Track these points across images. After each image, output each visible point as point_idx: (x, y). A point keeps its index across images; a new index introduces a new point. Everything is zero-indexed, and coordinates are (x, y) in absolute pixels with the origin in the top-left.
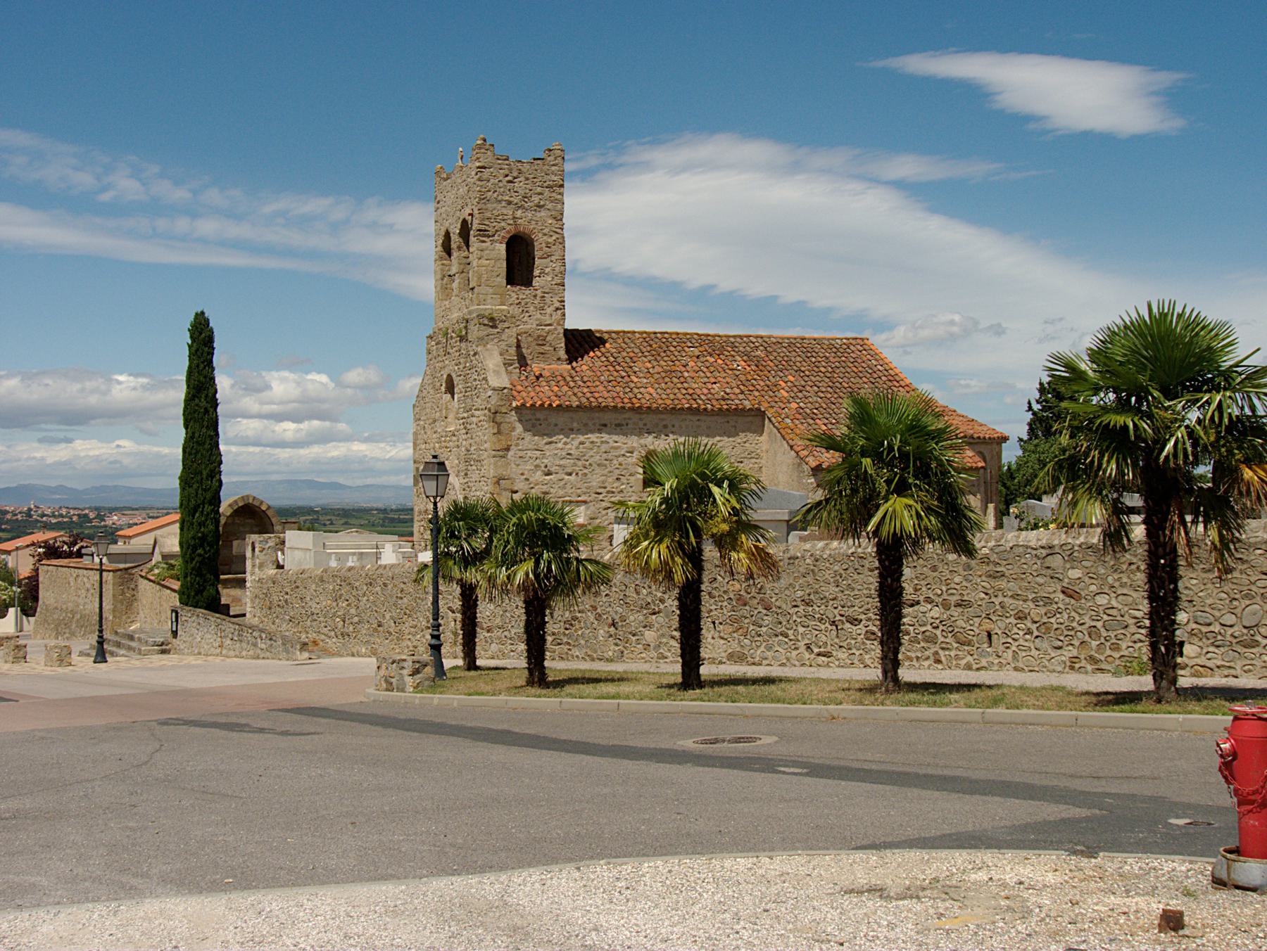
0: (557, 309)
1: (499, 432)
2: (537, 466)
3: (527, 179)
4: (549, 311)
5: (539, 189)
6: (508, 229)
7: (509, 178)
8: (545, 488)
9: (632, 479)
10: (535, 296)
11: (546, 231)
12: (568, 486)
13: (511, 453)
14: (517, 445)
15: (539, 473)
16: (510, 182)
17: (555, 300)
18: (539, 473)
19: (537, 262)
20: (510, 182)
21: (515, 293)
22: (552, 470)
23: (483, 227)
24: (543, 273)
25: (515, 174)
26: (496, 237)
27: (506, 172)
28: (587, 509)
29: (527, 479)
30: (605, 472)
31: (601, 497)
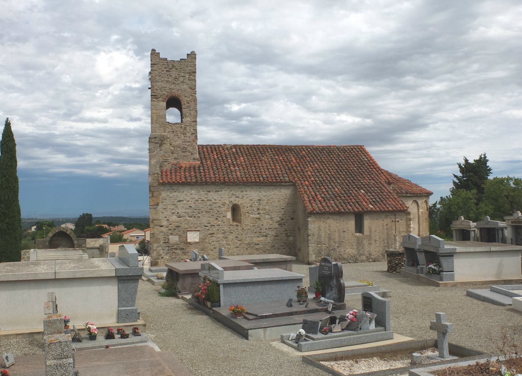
0: (193, 134)
1: (152, 196)
3: (177, 69)
4: (189, 135)
5: (183, 74)
8: (177, 224)
13: (159, 207)
14: (162, 202)
16: (167, 71)
20: (167, 71)
22: (182, 215)
31: (207, 228)
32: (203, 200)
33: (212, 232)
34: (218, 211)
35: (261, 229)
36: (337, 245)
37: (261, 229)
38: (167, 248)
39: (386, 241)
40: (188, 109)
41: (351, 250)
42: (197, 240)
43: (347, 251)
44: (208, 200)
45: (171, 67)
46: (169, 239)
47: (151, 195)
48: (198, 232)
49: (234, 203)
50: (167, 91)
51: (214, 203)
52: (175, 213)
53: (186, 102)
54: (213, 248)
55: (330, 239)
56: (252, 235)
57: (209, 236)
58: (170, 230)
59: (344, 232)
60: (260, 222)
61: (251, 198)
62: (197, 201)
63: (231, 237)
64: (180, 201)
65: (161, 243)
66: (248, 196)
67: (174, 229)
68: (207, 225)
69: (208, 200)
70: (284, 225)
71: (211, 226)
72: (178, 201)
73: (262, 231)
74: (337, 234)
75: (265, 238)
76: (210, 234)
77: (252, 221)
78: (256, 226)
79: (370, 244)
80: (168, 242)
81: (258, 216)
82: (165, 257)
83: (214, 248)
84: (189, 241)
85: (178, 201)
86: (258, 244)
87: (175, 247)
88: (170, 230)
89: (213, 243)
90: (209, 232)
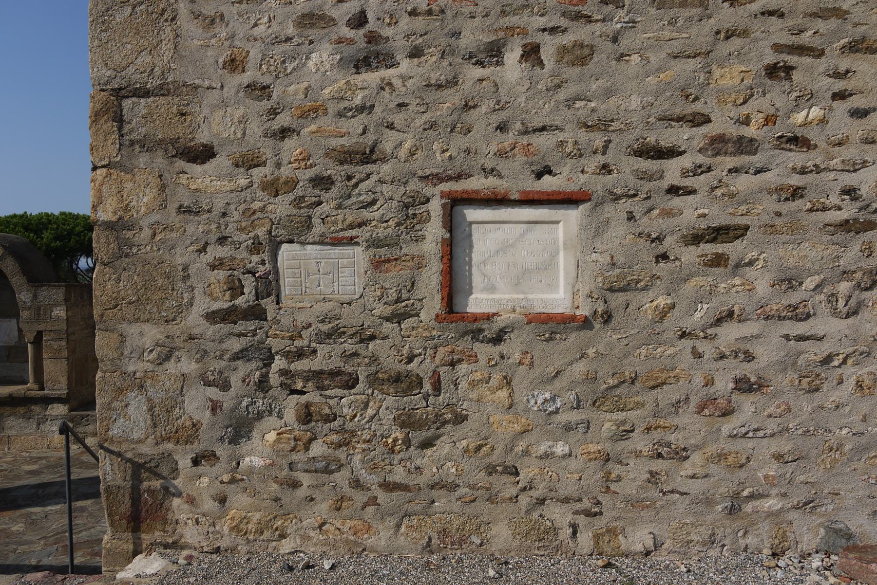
12: (482, 119)
18: (322, 57)
28: (596, 230)
30: (701, 34)
31: (673, 171)
33: (719, 215)
38: (249, 368)
42: (558, 297)
46: (269, 286)
48: (571, 219)
52: (326, 21)
54: (723, 385)
57: (690, 255)
58: (273, 188)
65: (194, 320)
67: (322, 182)
68: (667, 137)
71: (718, 144)
76: (696, 239)
80: (256, 313)
82: (223, 451)
84: (477, 302)
87: (325, 358)
88: (273, 188)
89: (730, 333)
90: (691, 212)
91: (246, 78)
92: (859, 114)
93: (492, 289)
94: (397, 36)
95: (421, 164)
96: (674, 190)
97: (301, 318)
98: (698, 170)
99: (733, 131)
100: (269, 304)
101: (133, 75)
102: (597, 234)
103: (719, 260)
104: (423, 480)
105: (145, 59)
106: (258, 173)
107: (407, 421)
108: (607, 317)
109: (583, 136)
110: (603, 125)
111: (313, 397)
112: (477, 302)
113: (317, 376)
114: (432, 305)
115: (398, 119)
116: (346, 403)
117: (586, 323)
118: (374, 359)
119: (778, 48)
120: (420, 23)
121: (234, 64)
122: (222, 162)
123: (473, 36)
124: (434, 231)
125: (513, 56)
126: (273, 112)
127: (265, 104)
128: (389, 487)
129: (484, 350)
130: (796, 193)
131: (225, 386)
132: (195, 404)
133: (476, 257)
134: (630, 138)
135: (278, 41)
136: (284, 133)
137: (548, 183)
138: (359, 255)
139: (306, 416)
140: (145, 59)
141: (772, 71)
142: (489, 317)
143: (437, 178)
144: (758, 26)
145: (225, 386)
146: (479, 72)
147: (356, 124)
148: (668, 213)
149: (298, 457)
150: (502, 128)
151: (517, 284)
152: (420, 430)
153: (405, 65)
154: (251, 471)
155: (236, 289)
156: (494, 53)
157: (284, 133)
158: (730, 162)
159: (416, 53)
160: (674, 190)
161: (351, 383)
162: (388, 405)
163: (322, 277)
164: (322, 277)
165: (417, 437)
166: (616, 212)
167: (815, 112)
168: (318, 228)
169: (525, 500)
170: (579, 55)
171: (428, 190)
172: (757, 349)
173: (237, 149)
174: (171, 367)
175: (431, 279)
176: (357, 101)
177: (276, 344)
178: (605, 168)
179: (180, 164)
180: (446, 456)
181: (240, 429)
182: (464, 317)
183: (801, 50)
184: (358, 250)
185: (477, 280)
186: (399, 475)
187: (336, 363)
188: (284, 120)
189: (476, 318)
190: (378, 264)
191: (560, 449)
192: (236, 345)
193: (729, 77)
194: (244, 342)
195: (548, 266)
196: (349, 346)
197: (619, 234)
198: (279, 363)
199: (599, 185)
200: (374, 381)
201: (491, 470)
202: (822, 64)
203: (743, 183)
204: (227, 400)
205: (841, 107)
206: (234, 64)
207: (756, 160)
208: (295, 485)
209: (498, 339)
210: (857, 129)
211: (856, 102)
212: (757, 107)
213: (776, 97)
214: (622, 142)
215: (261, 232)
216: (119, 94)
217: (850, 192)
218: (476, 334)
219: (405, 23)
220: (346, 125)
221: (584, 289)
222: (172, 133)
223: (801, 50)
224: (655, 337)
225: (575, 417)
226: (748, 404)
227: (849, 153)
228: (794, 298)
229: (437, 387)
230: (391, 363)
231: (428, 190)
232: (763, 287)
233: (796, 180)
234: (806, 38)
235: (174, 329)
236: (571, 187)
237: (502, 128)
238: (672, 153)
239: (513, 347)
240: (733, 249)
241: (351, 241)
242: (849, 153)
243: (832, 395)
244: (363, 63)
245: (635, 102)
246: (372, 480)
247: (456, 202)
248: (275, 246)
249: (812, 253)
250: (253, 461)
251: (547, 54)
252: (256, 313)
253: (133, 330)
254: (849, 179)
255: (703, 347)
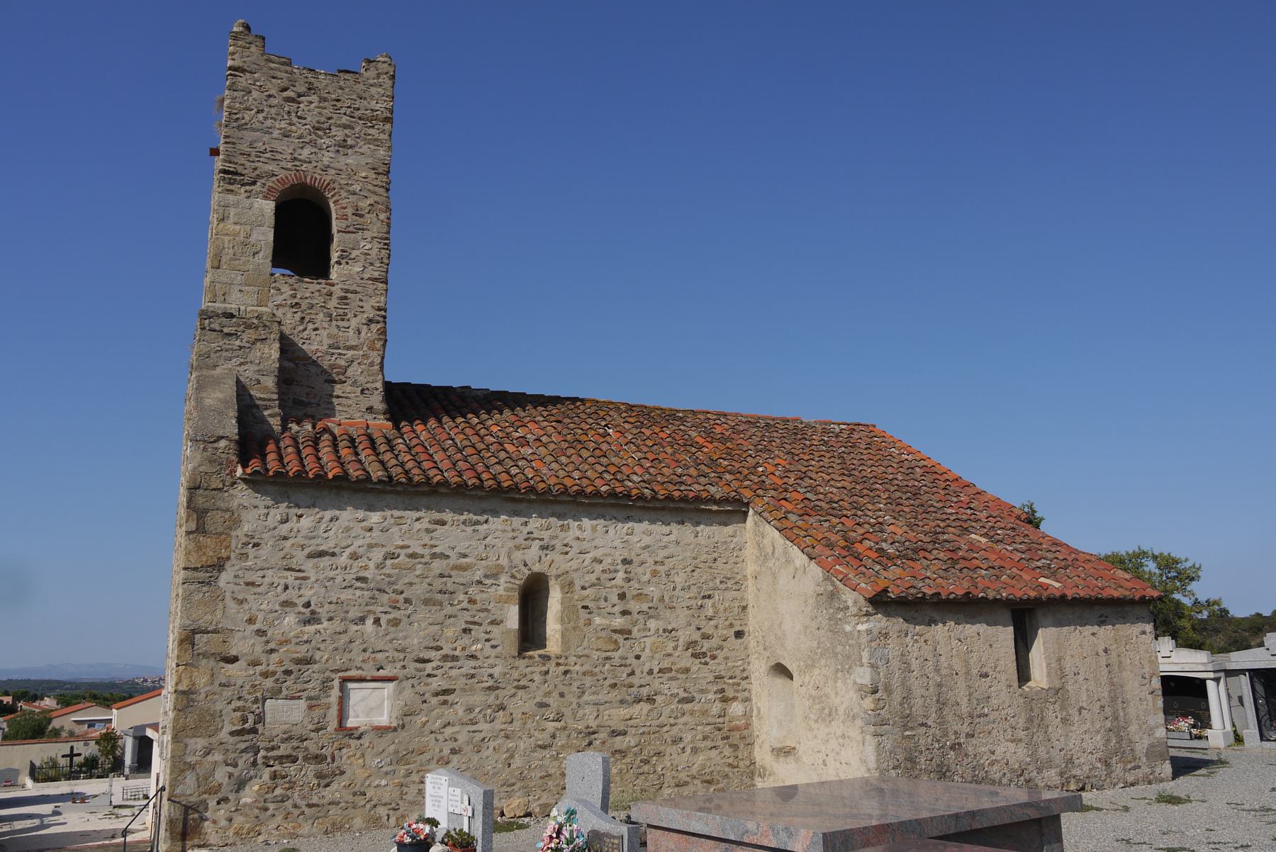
2: (287, 604)
5: (345, 120)
6: (281, 172)
7: (288, 94)
8: (302, 651)
9: (496, 630)
10: (330, 294)
11: (357, 187)
12: (357, 646)
13: (225, 578)
15: (290, 620)
17: (367, 307)
18: (290, 620)
19: (336, 238)
21: (287, 286)
23: (231, 167)
24: (345, 256)
25: (302, 89)
26: (257, 187)
27: (285, 83)
28: (400, 691)
29: (260, 633)
30: (439, 616)
31: (429, 667)
32: (413, 556)
33: (445, 685)
34: (472, 601)
35: (632, 673)
36: (966, 729)
37: (632, 673)
38: (249, 757)
39: (1108, 710)
40: (359, 235)
41: (1012, 746)
42: (384, 719)
43: (1000, 750)
44: (434, 556)
45: (302, 88)
46: (260, 719)
47: (193, 526)
48: (391, 685)
49: (537, 568)
50: (284, 164)
51: (455, 567)
52: (293, 605)
53: (349, 211)
54: (446, 752)
55: (942, 704)
56: (601, 697)
57: (434, 701)
58: (265, 675)
59: (986, 676)
60: (628, 643)
61: (598, 553)
62: (393, 556)
63: (521, 704)
64: (321, 554)
65: (224, 735)
66: (585, 545)
69: (434, 556)
70: (714, 657)
71: (445, 658)
72: (310, 556)
73: (636, 680)
74: (961, 683)
75: (645, 707)
76: (437, 694)
77: (601, 644)
78: (617, 661)
79: (1065, 721)
80: (254, 731)
81: (619, 622)
82: (232, 797)
83: (454, 752)
84: (351, 723)
85: (310, 556)
86: (624, 733)
87: (284, 750)
88: (265, 675)
89: (449, 730)
90: (436, 684)
91: (256, 627)
92: (494, 647)
93: (357, 716)
94: (323, 612)
95: (331, 666)
96: (429, 675)
97: (274, 733)
98: (438, 668)
99: (451, 653)
100: (260, 727)
101: (202, 624)
102: (400, 693)
103: (445, 702)
104: (325, 801)
105: (208, 617)
106: (259, 668)
107: (319, 776)
108: (403, 727)
109: (396, 654)
110: (403, 650)
111: (277, 767)
112: (351, 723)
113: (281, 759)
114: (333, 724)
115: (322, 646)
116: (292, 769)
117: (395, 729)
118: (306, 749)
119: (467, 622)
120: (333, 607)
121: (251, 621)
122: (241, 664)
123: (354, 613)
124: (335, 693)
125: (369, 621)
126: (267, 642)
127: (264, 638)
128: (309, 806)
129: (353, 743)
130: (473, 676)
131: (236, 766)
132: (221, 775)
133: (351, 703)
134: (414, 655)
135: (271, 612)
136: (272, 651)
137: (382, 673)
138: (302, 704)
139: (274, 776)
140: (208, 617)
141: (465, 631)
142: (357, 728)
143: (338, 671)
144: (460, 614)
145: (236, 766)
146: (356, 628)
147: (305, 647)
148: (427, 684)
149: (269, 796)
150: (364, 650)
151: (368, 715)
152: (325, 779)
153: (326, 624)
154: (245, 805)
155: (245, 720)
156: (362, 620)
157: (272, 651)
158: (449, 664)
159: (330, 619)
160: (429, 675)
161: (295, 760)
162: (311, 769)
163: (285, 714)
164: (285, 714)
165: (323, 782)
166: (408, 684)
167: (479, 646)
168: (285, 692)
169: (368, 806)
170: (395, 623)
171: (333, 676)
172: (459, 737)
173: (250, 658)
174: (210, 758)
175: (333, 712)
176: (305, 638)
177: (262, 745)
178: (404, 667)
179: (222, 664)
180: (335, 790)
181: (241, 785)
182: (346, 729)
183: (474, 623)
184: (302, 701)
185: (351, 713)
186: (315, 800)
187: (289, 752)
188: (272, 645)
189: (351, 729)
190: (310, 707)
191: (383, 782)
192: (243, 746)
193: (450, 632)
194: (247, 744)
195: (380, 706)
196: (295, 744)
197: (408, 693)
198: (262, 753)
199: (401, 673)
200: (306, 759)
201: (355, 794)
202: (482, 629)
203: (454, 672)
204: (236, 772)
205: (488, 644)
206: (251, 621)
207: (459, 664)
208: (266, 809)
209: (359, 738)
210: (494, 652)
211: (493, 643)
212: (459, 644)
213: (466, 640)
214: (410, 657)
215: (259, 694)
216: (194, 632)
217: (491, 676)
218: (350, 736)
219: (327, 606)
220: (299, 648)
221: (394, 715)
222: (219, 650)
223: (474, 623)
224: (421, 734)
225: (389, 768)
226: (455, 758)
227: (491, 661)
228: (472, 716)
229: (333, 760)
230: (314, 750)
231: (333, 676)
232: (461, 712)
233: (473, 671)
234: (476, 619)
235: (213, 740)
236: (390, 675)
237: (364, 650)
238: (429, 661)
239: (365, 741)
240: (450, 698)
241: (299, 698)
242: (491, 661)
243: (485, 753)
244: (307, 622)
245: (416, 641)
246: (302, 803)
247: (345, 680)
248: (264, 700)
249: (478, 699)
250: (247, 800)
251: (383, 622)
252: (254, 731)
253: (193, 740)
254: (491, 671)
255: (440, 737)
